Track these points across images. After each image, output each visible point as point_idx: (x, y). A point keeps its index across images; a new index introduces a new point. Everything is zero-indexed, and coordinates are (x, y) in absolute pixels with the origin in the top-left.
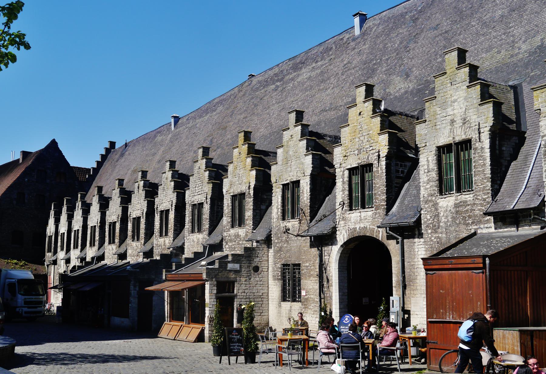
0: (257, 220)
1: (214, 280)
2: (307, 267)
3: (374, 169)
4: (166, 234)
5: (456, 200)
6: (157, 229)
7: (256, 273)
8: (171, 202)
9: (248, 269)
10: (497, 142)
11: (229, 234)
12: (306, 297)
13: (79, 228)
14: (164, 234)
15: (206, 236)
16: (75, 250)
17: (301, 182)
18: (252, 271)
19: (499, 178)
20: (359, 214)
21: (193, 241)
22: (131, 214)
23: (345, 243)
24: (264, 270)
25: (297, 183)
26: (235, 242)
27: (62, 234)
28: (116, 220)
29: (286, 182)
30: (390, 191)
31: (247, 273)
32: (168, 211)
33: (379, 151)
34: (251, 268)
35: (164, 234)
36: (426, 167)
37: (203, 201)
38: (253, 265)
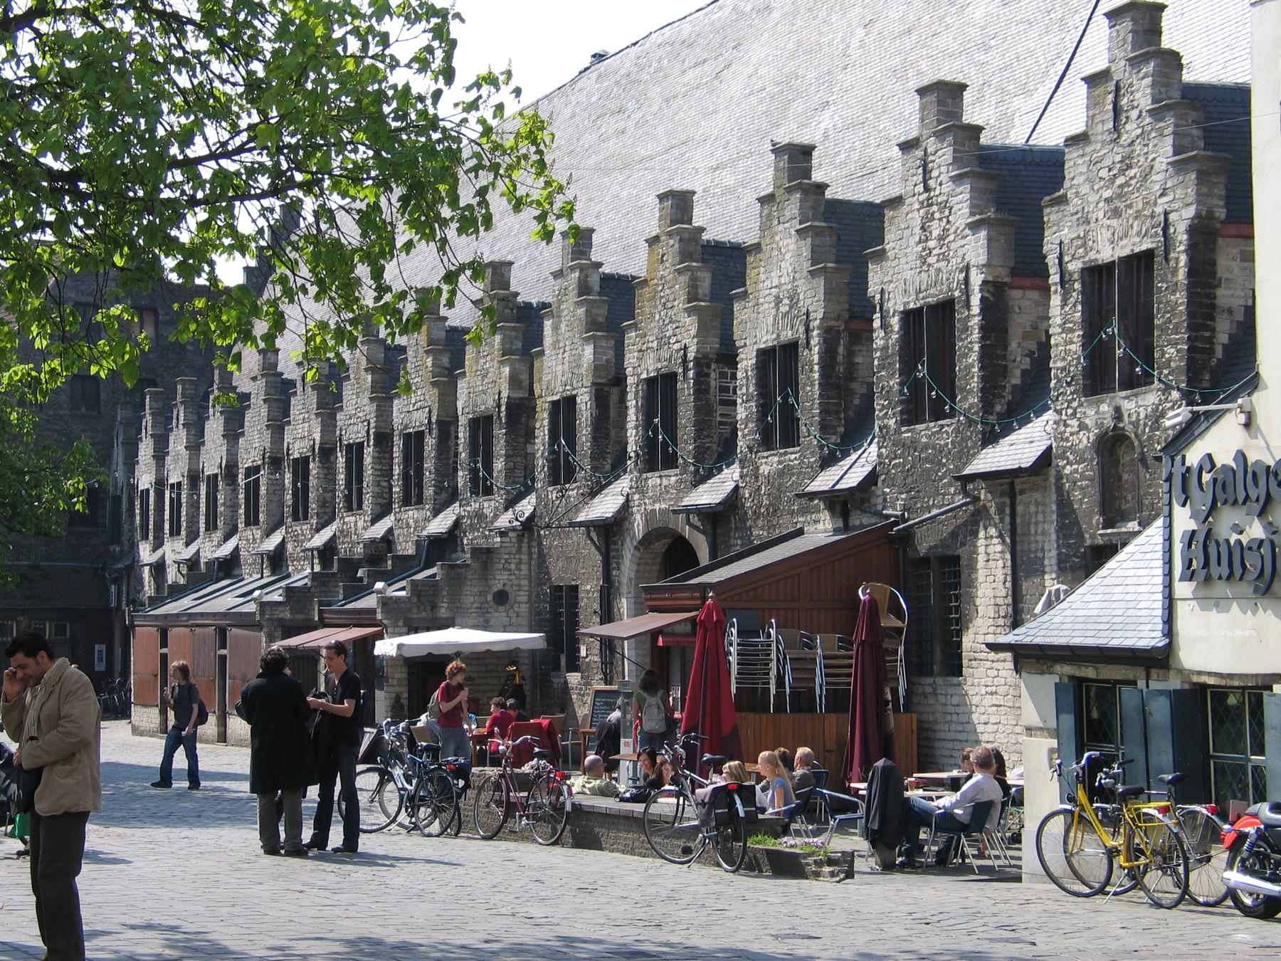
0: (517, 479)
1: (401, 623)
2: (588, 592)
3: (679, 385)
4: (360, 507)
5: (780, 462)
6: (342, 492)
7: (501, 608)
8: (366, 424)
9: (483, 599)
10: (841, 350)
11: (468, 512)
12: (587, 660)
13: (181, 479)
14: (355, 506)
15: (428, 513)
16: (175, 538)
17: (578, 400)
18: (492, 603)
19: (843, 421)
20: (658, 481)
21: (408, 526)
22: (291, 446)
23: (640, 542)
24: (519, 599)
25: (571, 401)
26: (478, 531)
27: (142, 491)
28: (259, 463)
29: (556, 398)
30: (705, 433)
31: (481, 608)
32: (360, 446)
33: (686, 348)
34: (490, 597)
35: (355, 506)
36: (744, 390)
37: (423, 428)
38: (495, 589)
